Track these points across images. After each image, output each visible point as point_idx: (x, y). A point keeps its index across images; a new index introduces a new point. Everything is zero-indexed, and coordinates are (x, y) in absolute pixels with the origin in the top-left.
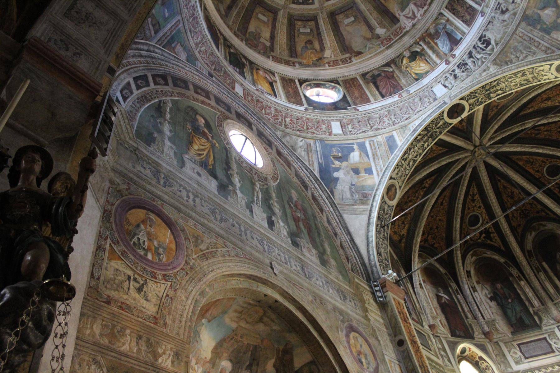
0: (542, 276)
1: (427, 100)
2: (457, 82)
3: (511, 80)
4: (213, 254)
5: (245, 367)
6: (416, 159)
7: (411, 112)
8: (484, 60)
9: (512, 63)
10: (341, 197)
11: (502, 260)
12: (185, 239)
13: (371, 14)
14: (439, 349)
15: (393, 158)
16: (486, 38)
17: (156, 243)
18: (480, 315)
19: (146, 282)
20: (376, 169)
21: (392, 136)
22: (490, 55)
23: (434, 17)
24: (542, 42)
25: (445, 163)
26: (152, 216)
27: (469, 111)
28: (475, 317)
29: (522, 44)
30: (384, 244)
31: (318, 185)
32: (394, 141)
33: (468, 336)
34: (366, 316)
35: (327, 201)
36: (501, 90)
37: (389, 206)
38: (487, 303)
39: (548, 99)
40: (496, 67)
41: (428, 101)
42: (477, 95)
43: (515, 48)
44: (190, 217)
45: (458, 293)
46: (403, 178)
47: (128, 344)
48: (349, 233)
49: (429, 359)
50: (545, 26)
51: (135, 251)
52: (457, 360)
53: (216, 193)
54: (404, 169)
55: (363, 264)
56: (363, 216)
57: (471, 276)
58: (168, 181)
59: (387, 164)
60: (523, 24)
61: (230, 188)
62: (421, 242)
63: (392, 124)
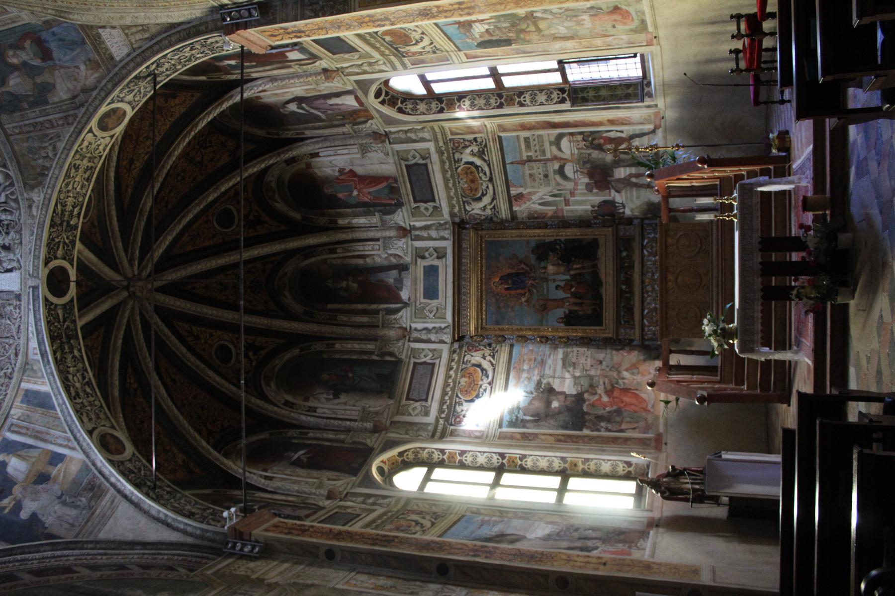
0: (343, 318)
1: (9, 308)
2: (17, 251)
3: (70, 187)
6: (87, 380)
7: (11, 341)
8: (13, 197)
9: (48, 169)
10: (67, 526)
11: (297, 351)
14: (363, 502)
15: (62, 411)
18: (348, 423)
20: (61, 445)
21: (27, 391)
22: (12, 184)
25: (120, 342)
27: (72, 265)
28: (348, 431)
29: (33, 139)
30: (180, 499)
32: (37, 393)
33: (367, 454)
34: (269, 585)
36: (74, 207)
37: (130, 460)
38: (338, 404)
39: (132, 162)
40: (36, 190)
41: (12, 307)
42: (57, 240)
43: (30, 150)
45: (306, 434)
46: (102, 416)
48: (133, 544)
49: (368, 525)
50: (31, 99)
52: (388, 487)
54: (91, 405)
55: (191, 547)
56: (120, 508)
57: (293, 404)
59: (65, 425)
62: (208, 443)
63: (7, 380)
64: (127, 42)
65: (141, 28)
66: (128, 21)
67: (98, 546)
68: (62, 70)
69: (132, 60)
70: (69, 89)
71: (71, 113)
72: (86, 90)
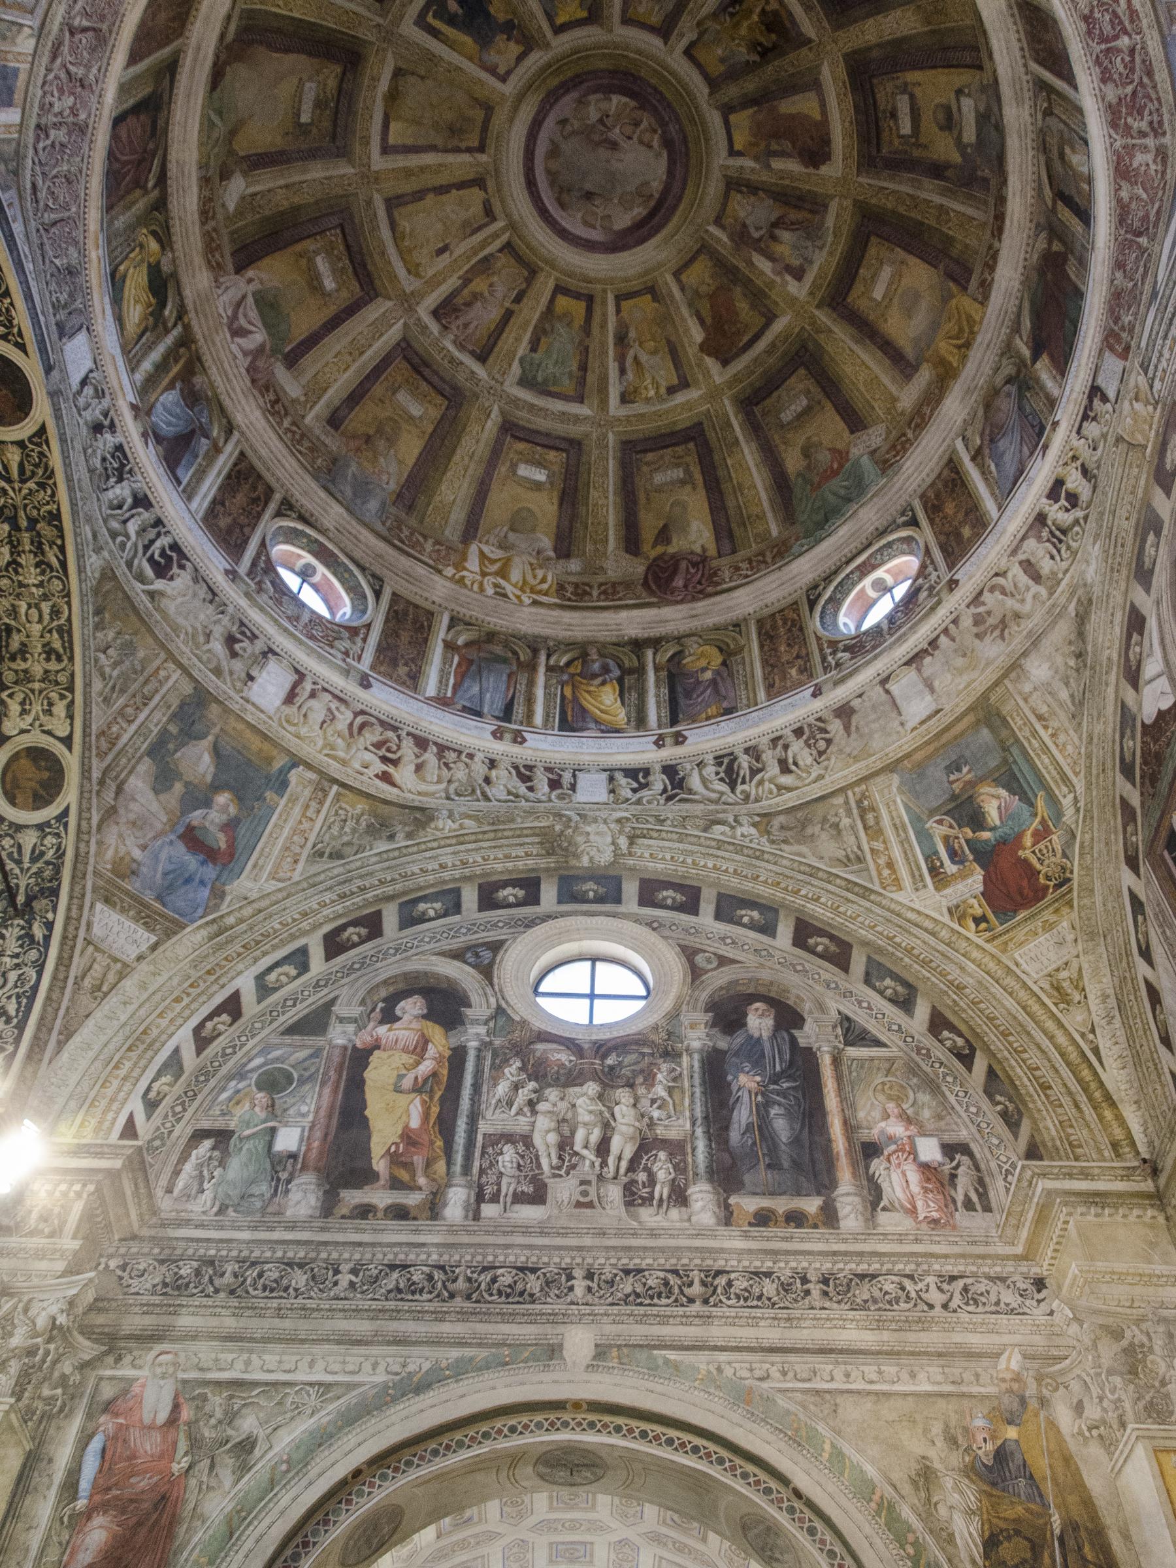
13: (287, 186)
16: (175, 570)
23: (227, 403)
24: (134, 727)
50: (171, 746)
60: (187, 688)
64: (102, 946)
65: (105, 988)
66: (128, 984)
68: (159, 826)
69: (79, 919)
70: (134, 799)
71: (110, 758)
72: (110, 813)
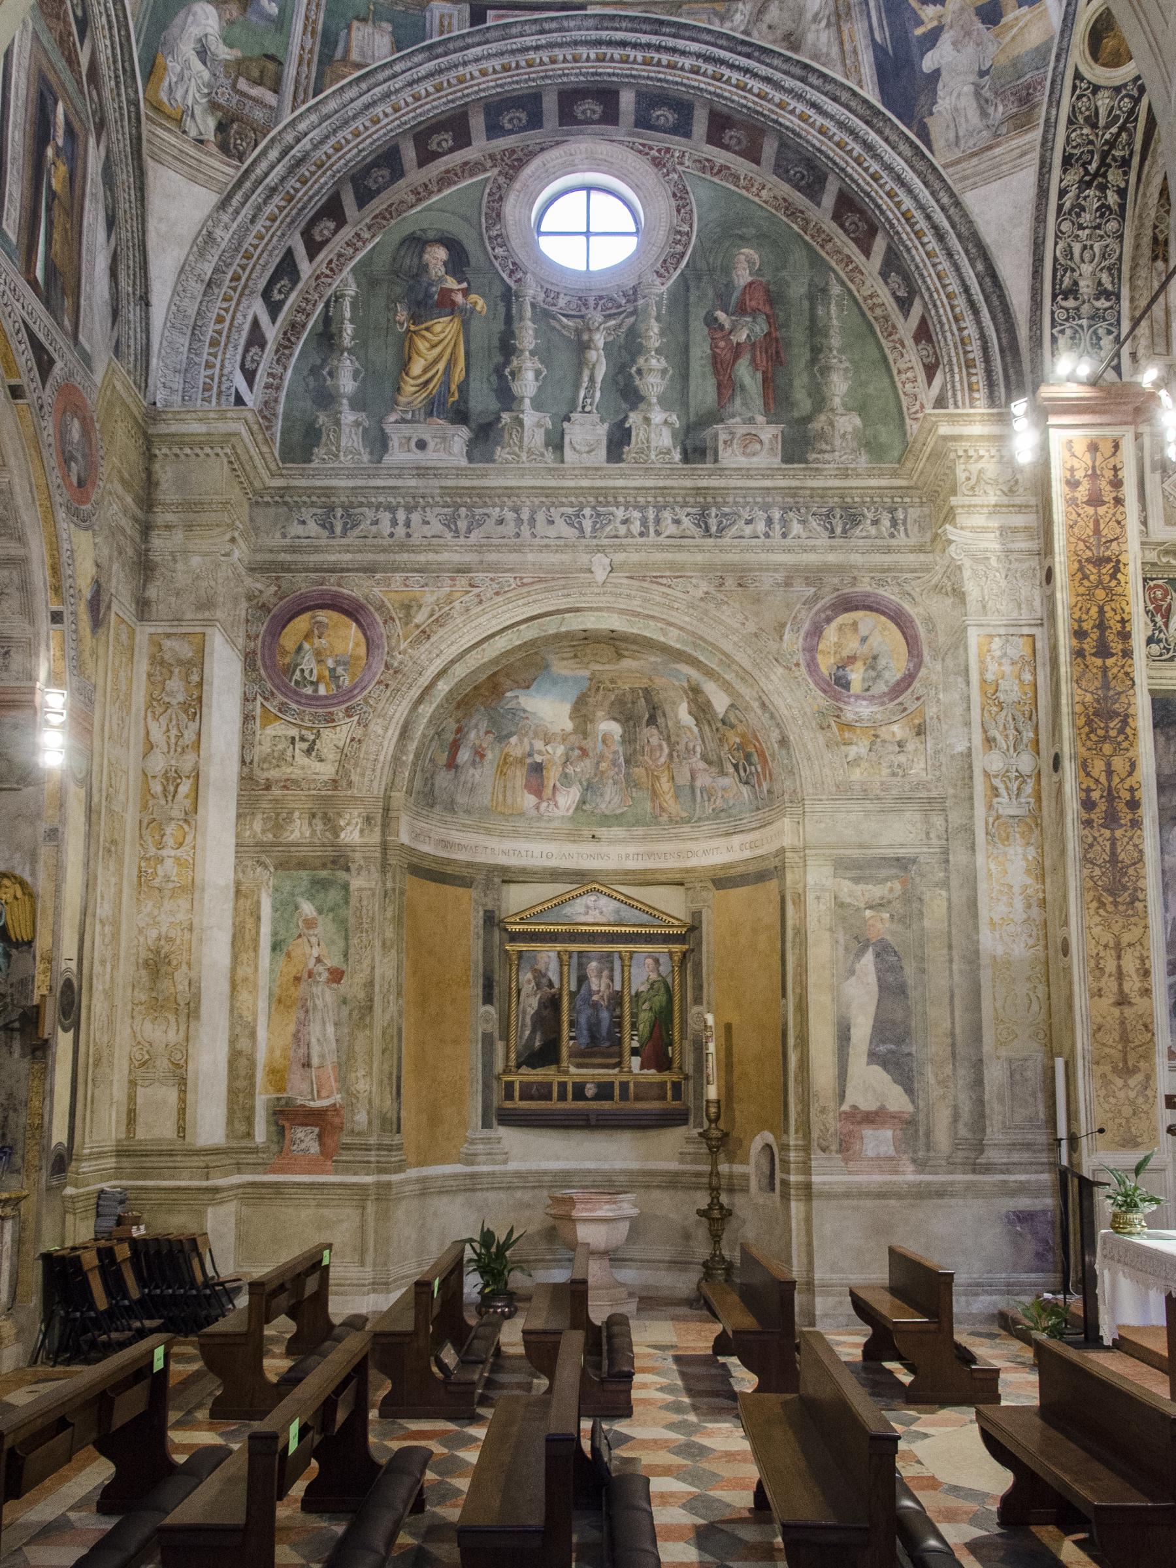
4: (440, 622)
5: (644, 722)
10: (952, 135)
12: (385, 622)
17: (330, 663)
19: (318, 735)
26: (323, 616)
31: (879, 132)
35: (910, 175)
44: (395, 570)
47: (298, 831)
51: (297, 693)
53: (464, 462)
56: (1021, 174)
58: (349, 516)
61: (506, 417)
67: (952, 211)
